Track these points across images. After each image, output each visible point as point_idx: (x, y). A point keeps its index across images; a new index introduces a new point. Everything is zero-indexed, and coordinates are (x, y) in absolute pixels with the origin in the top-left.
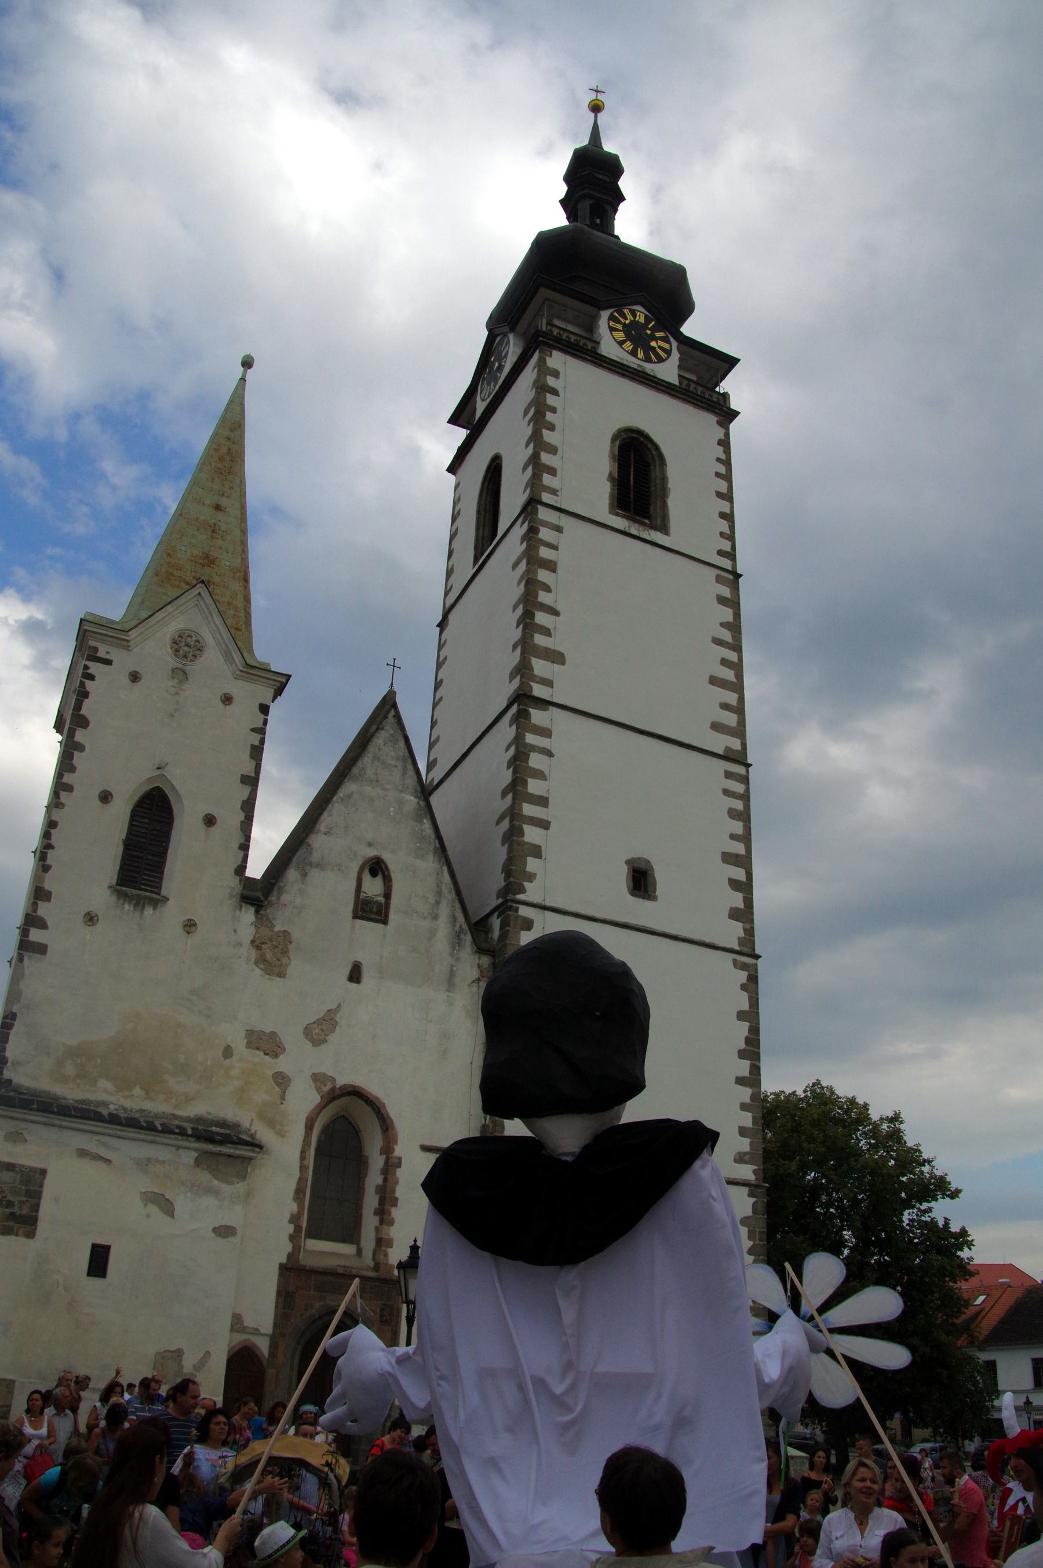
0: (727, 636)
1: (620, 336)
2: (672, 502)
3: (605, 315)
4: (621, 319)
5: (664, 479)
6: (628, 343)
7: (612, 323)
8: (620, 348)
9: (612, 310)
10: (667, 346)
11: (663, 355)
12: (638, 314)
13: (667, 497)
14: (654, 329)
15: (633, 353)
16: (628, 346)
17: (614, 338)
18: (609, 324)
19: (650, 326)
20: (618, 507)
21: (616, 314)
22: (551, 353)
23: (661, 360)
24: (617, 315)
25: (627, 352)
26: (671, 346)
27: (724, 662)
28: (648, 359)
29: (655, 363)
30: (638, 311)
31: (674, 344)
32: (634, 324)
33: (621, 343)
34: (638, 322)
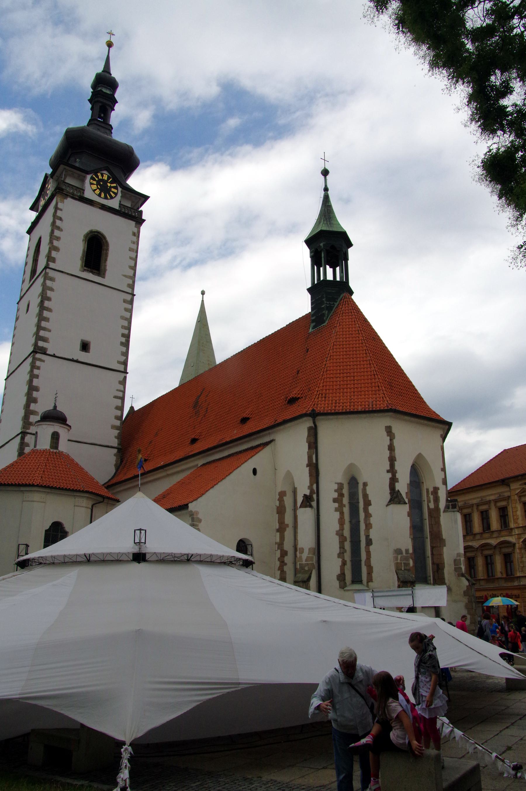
1: (95, 187)
3: (89, 177)
4: (96, 178)
6: (98, 190)
7: (92, 181)
8: (93, 193)
9: (93, 174)
10: (116, 191)
11: (113, 195)
12: (104, 175)
15: (99, 195)
16: (98, 192)
18: (90, 181)
20: (85, 266)
21: (94, 176)
23: (112, 198)
24: (94, 177)
25: (97, 194)
26: (118, 191)
28: (106, 198)
29: (109, 199)
30: (105, 174)
31: (120, 189)
32: (102, 180)
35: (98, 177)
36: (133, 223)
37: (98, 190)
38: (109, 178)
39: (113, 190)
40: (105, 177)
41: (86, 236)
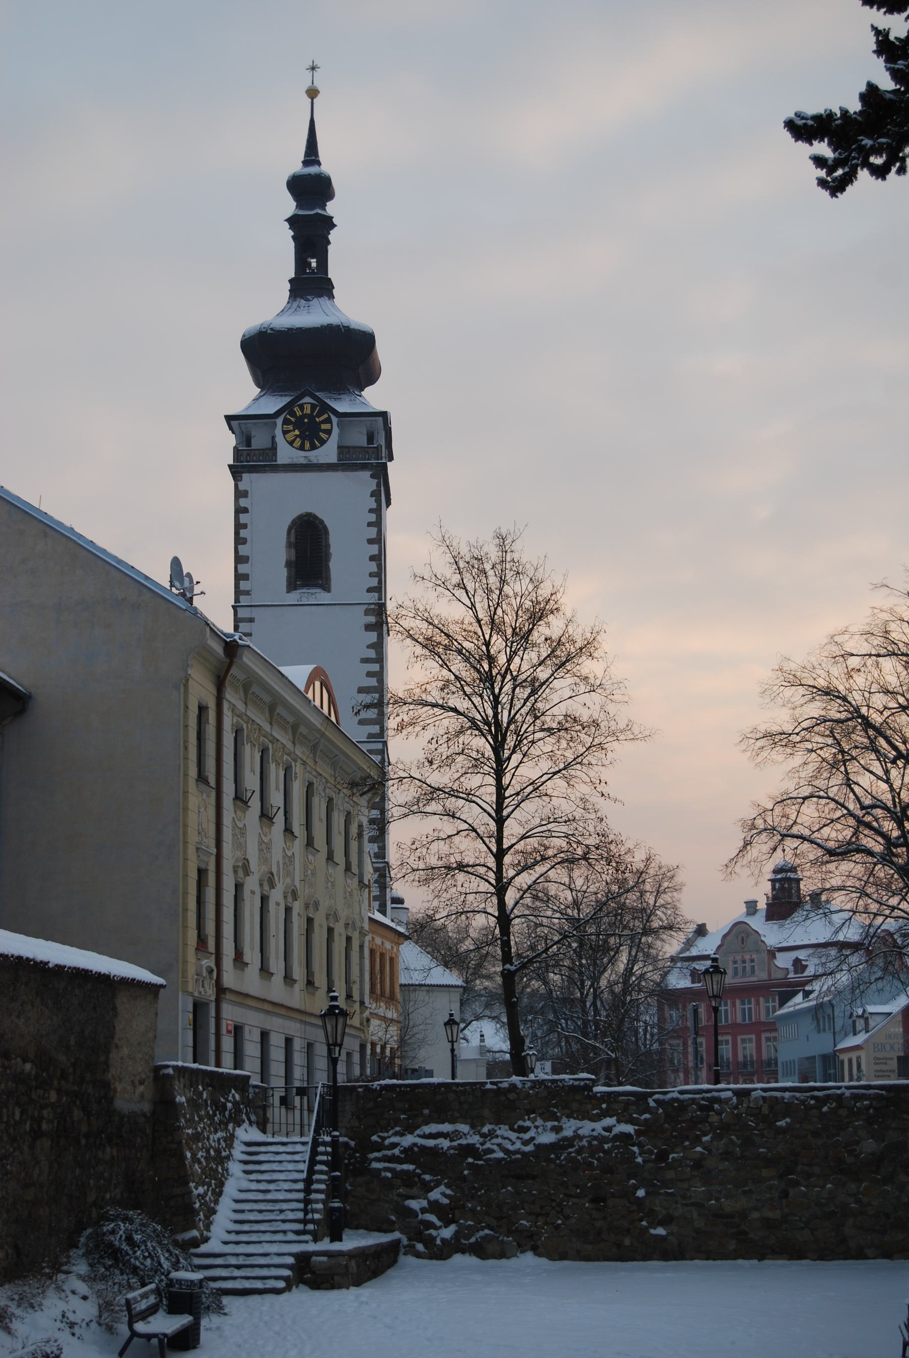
0: (372, 654)
2: (332, 565)
3: (280, 421)
4: (292, 419)
5: (328, 546)
13: (329, 561)
14: (319, 415)
15: (302, 448)
22: (241, 477)
23: (323, 442)
25: (297, 448)
26: (332, 425)
27: (369, 674)
28: (313, 447)
31: (335, 420)
32: (304, 416)
33: (291, 443)
35: (293, 414)
36: (366, 474)
38: (313, 407)
39: (324, 427)
40: (308, 410)
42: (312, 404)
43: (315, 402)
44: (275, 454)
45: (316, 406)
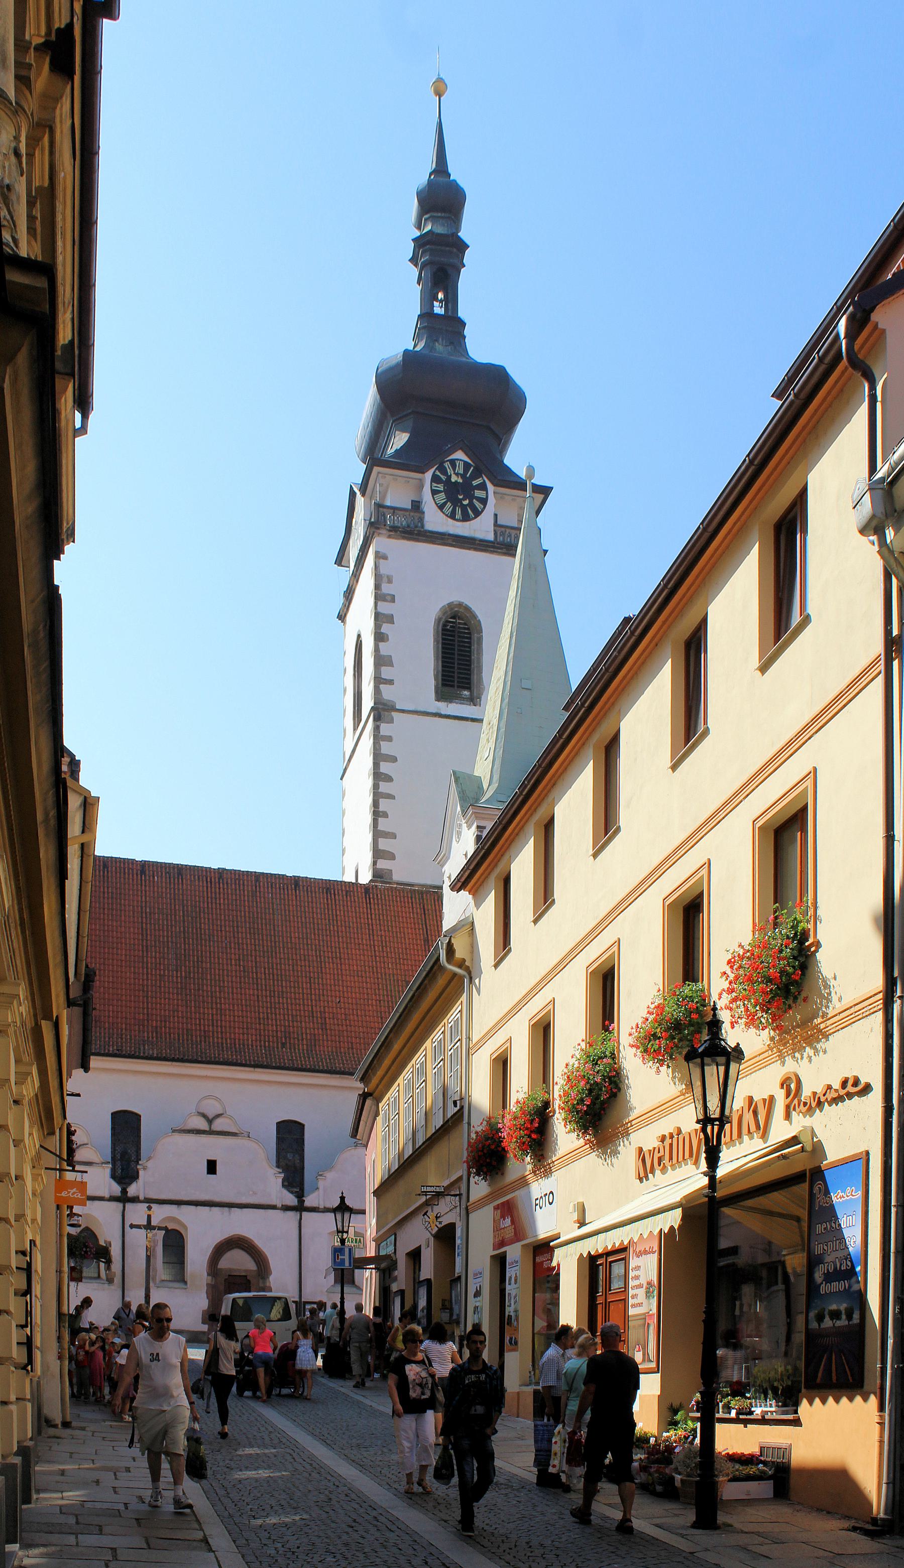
1: (441, 498)
4: (442, 476)
6: (449, 504)
17: (436, 503)
19: (472, 468)
21: (438, 473)
30: (457, 460)
33: (441, 507)
34: (447, 498)
37: (449, 504)
38: (467, 466)
41: (444, 610)
42: (465, 463)
43: (470, 461)
44: (421, 520)
45: (470, 465)
